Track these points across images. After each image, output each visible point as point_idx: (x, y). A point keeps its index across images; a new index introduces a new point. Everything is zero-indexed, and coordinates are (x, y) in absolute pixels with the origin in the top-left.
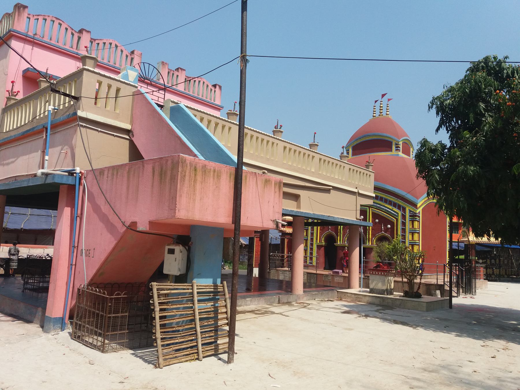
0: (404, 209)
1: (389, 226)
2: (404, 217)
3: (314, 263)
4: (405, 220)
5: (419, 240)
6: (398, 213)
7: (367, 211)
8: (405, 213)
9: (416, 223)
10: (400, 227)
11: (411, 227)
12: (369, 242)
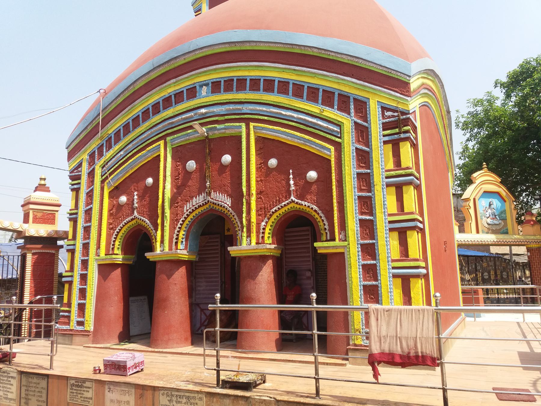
0: (362, 107)
1: (312, 175)
2: (362, 133)
3: (90, 326)
4: (368, 143)
5: (421, 214)
6: (339, 125)
7: (240, 137)
8: (365, 118)
9: (406, 149)
10: (350, 169)
11: (391, 165)
12: (249, 236)
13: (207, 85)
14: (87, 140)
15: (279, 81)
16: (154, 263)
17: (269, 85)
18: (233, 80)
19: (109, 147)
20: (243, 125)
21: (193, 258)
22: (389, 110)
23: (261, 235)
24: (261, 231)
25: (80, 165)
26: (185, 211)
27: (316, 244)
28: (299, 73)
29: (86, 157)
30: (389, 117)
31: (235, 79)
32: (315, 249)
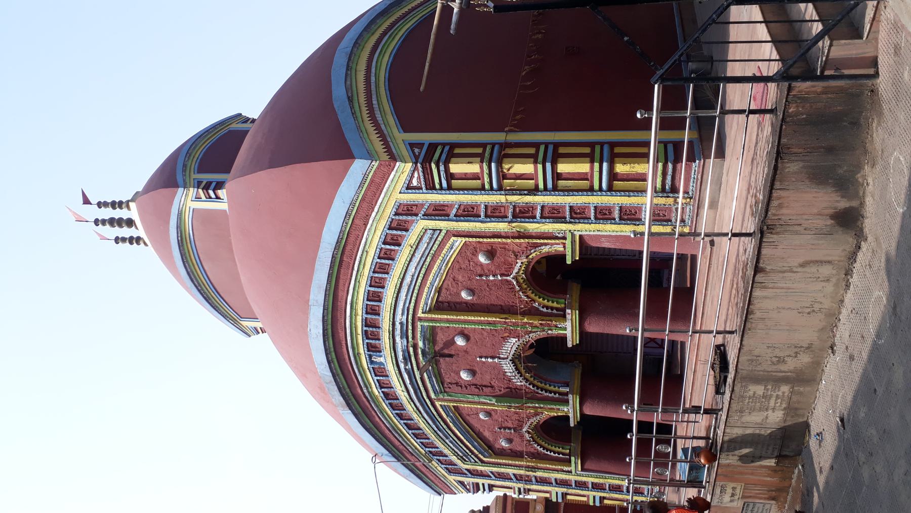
14: (439, 487)
15: (370, 286)
16: (582, 415)
17: (374, 297)
18: (366, 331)
21: (578, 372)
22: (410, 181)
23: (555, 311)
24: (549, 311)
25: (462, 483)
27: (569, 262)
28: (362, 266)
29: (452, 478)
30: (419, 182)
31: (365, 328)
32: (574, 262)
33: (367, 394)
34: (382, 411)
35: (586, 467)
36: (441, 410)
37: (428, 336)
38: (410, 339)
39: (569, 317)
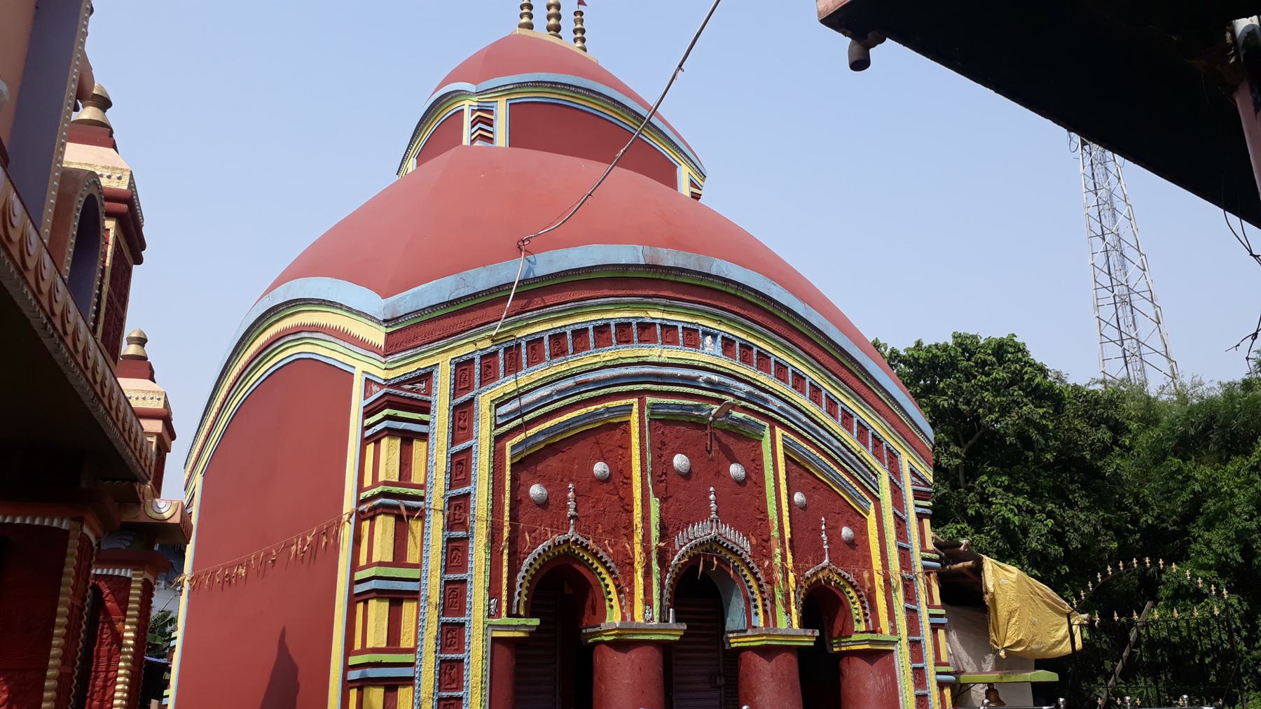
13: (714, 336)
19: (513, 367)
20: (768, 425)
26: (677, 547)
33: (656, 300)
34: (618, 306)
35: (497, 646)
36: (623, 402)
37: (741, 428)
38: (743, 403)
39: (809, 632)
